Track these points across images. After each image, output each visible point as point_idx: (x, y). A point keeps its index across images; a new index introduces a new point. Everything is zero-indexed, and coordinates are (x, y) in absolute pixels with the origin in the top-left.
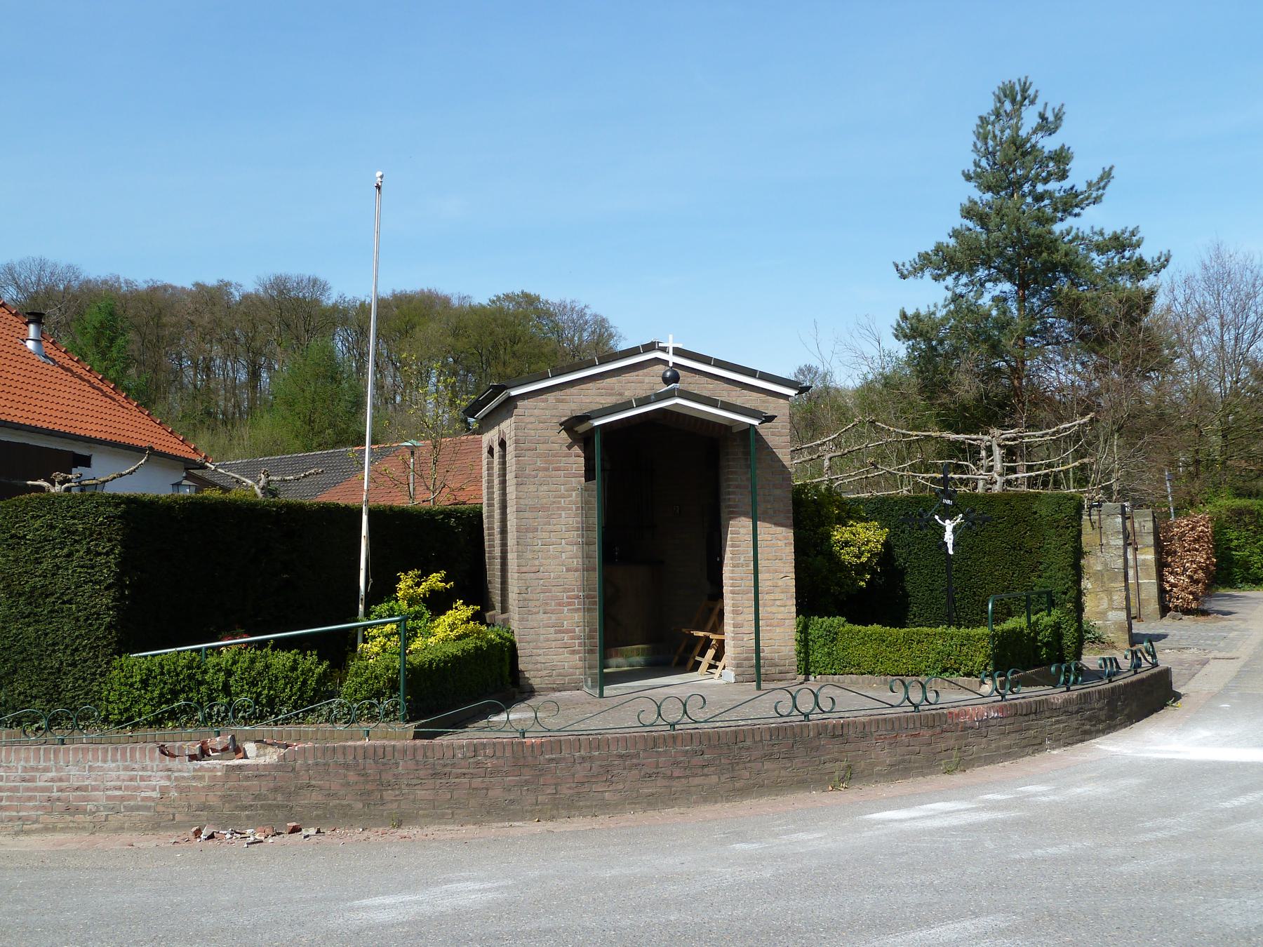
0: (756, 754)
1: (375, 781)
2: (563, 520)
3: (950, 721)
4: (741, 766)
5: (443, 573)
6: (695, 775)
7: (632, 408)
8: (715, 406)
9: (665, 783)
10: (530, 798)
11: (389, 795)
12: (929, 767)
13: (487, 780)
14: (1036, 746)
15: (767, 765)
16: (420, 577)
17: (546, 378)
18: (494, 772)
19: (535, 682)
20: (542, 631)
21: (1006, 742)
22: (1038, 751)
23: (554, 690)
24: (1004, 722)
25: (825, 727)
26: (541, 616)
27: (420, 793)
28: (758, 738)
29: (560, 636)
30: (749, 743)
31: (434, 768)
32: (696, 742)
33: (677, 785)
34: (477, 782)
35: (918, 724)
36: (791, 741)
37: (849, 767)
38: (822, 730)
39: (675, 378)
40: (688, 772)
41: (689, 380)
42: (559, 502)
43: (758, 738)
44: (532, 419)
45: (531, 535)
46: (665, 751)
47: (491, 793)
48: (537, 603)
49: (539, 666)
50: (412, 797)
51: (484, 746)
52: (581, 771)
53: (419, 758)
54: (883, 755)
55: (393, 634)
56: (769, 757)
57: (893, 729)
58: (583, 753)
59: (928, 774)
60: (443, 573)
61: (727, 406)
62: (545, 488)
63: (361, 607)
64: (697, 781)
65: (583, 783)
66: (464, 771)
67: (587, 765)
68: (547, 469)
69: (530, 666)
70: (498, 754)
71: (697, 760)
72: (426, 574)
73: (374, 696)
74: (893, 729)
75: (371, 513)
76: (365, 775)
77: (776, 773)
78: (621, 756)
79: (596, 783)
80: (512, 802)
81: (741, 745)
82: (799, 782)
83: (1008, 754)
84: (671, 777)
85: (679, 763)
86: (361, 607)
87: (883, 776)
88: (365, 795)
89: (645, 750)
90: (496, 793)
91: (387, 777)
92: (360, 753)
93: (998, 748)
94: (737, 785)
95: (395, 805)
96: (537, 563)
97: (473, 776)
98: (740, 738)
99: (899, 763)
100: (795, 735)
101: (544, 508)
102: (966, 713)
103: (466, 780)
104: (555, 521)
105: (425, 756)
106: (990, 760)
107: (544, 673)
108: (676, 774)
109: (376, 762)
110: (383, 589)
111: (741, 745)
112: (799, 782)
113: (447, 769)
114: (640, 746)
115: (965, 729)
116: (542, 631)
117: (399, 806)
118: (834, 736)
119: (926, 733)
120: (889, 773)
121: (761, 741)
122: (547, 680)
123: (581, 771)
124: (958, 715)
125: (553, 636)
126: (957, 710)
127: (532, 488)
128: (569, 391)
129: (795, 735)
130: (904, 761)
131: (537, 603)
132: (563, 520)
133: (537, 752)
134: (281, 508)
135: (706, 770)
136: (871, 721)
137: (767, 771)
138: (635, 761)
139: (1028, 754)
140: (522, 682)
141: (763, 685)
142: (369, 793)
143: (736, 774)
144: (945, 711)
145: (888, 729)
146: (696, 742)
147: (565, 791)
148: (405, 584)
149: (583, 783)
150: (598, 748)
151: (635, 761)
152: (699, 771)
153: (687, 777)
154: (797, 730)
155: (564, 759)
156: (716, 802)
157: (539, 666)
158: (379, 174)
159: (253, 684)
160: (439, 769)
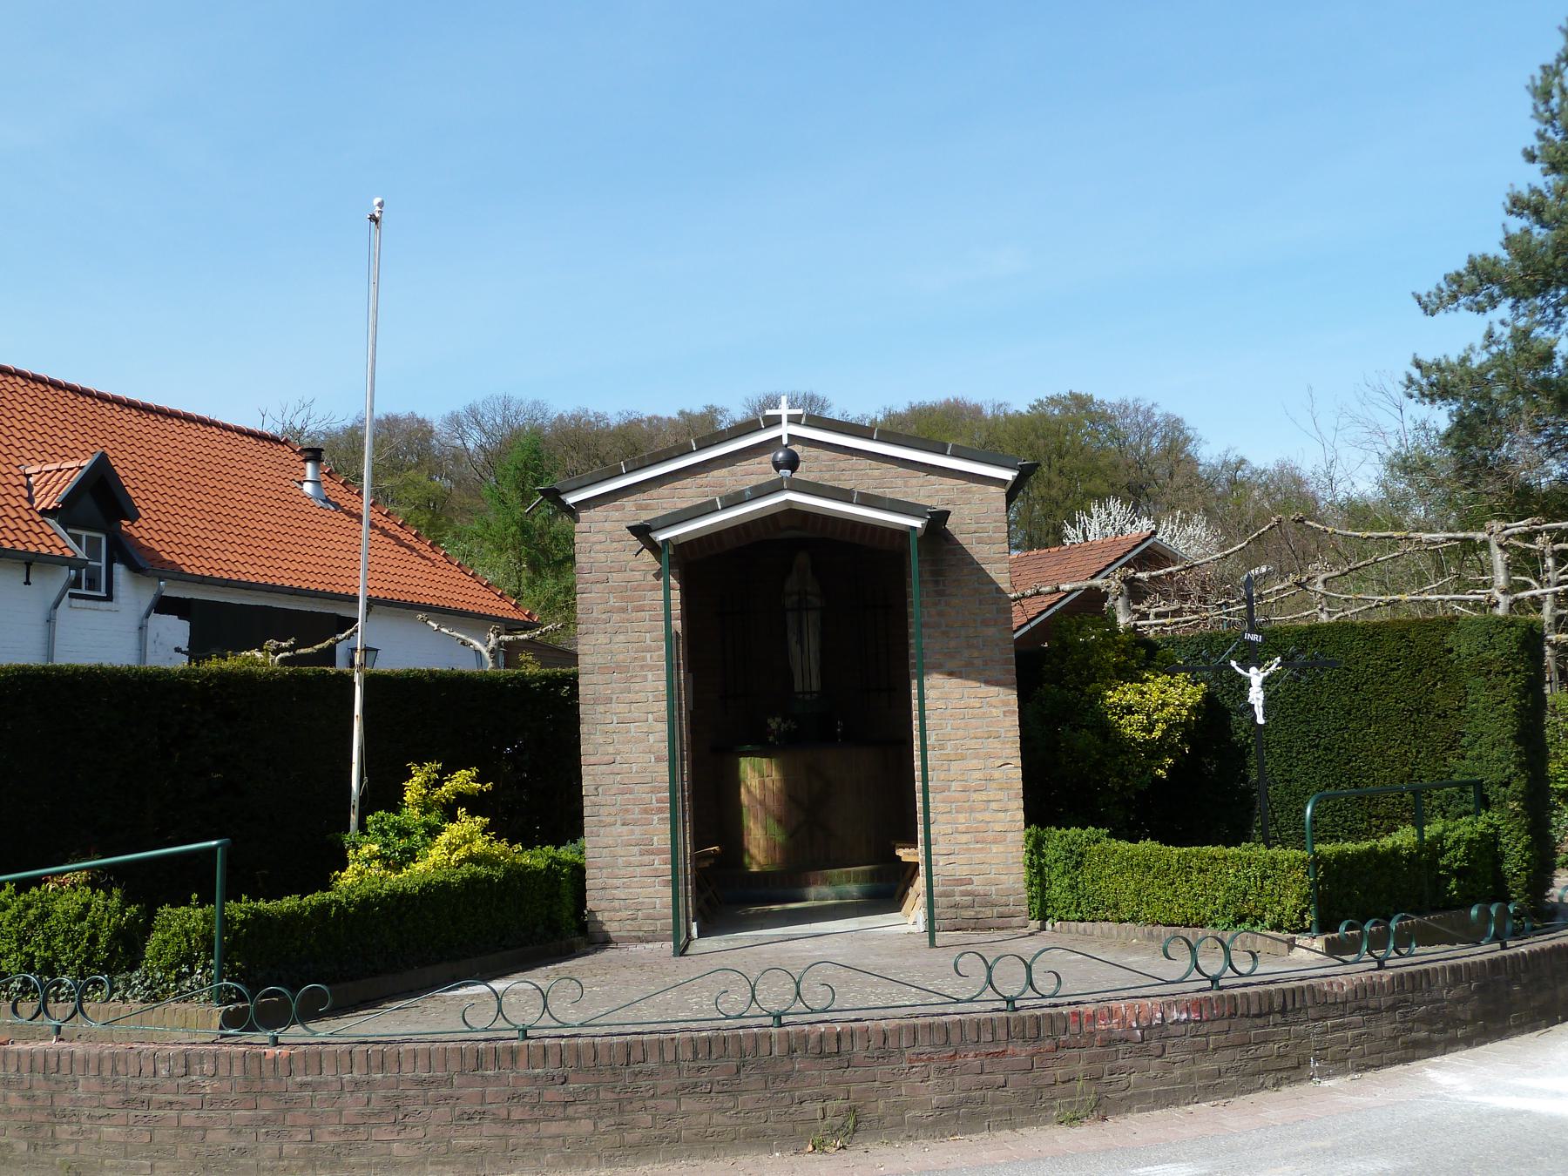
0: (664, 1084)
1: (43, 1108)
2: (650, 685)
3: (1074, 1028)
4: (637, 1105)
5: (474, 771)
6: (552, 1119)
7: (715, 511)
8: (849, 501)
9: (498, 1129)
10: (269, 1148)
11: (64, 1131)
12: (1026, 1112)
13: (203, 1114)
14: (1289, 1070)
15: (687, 1104)
16: (441, 773)
17: (618, 474)
18: (215, 1102)
19: (612, 928)
20: (620, 851)
21: (1207, 1066)
22: (1290, 1081)
23: (641, 940)
24: (1205, 1028)
25: (805, 1037)
26: (619, 829)
27: (108, 1131)
28: (669, 1056)
29: (646, 859)
30: (652, 1063)
31: (126, 1092)
32: (553, 1059)
33: (518, 1135)
34: (189, 1117)
35: (1002, 1034)
36: (734, 1063)
37: (853, 1110)
38: (796, 1046)
39: (792, 462)
40: (538, 1113)
41: (842, 465)
42: (644, 659)
43: (669, 1056)
44: (601, 537)
45: (601, 708)
46: (497, 1077)
47: (210, 1136)
48: (613, 810)
49: (616, 904)
50: (95, 1136)
51: (201, 1057)
52: (352, 1106)
53: (106, 1073)
54: (930, 1092)
55: (374, 857)
56: (690, 1089)
57: (947, 1042)
58: (356, 1074)
59: (1023, 1125)
60: (474, 771)
61: (867, 501)
62: (621, 637)
63: (354, 818)
64: (554, 1128)
65: (356, 1126)
66: (170, 1097)
67: (362, 1096)
68: (624, 610)
69: (604, 905)
70: (222, 1072)
71: (554, 1093)
72: (449, 769)
73: (183, 960)
74: (947, 1042)
75: (372, 682)
76: (32, 1098)
77: (705, 1117)
78: (421, 1082)
79: (378, 1125)
80: (243, 1152)
81: (637, 1068)
82: (748, 1135)
83: (1215, 1087)
84: (507, 1120)
85: (521, 1096)
86: (354, 818)
87: (919, 1126)
88: (32, 1128)
89: (461, 1072)
90: (218, 1136)
91: (62, 1102)
92: (25, 1063)
93: (1189, 1077)
94: (628, 1138)
95: (71, 1149)
96: (611, 749)
97: (184, 1106)
98: (637, 1054)
99: (961, 1104)
100: (742, 1054)
101: (620, 668)
102: (1112, 1014)
103: (173, 1113)
104: (637, 687)
105: (114, 1071)
106: (1168, 1098)
107: (624, 914)
108: (515, 1116)
109: (47, 1079)
110: (385, 794)
111: (637, 1068)
112: (748, 1135)
113: (145, 1094)
114: (454, 1066)
115: (1109, 1042)
116: (620, 851)
117: (76, 1152)
118: (821, 1055)
119: (1021, 1051)
120: (935, 1124)
121: (676, 1060)
122: (628, 925)
123: (352, 1106)
124: (1092, 1018)
125: (636, 859)
126: (1091, 1008)
127: (602, 639)
128: (655, 493)
129: (742, 1054)
130: (968, 1101)
131: (613, 810)
132: (650, 685)
133: (282, 1071)
134: (209, 679)
135: (570, 1111)
136: (900, 1028)
137: (686, 1115)
138: (444, 1091)
139: (1263, 1087)
140: (591, 928)
141: (941, 938)
142: (38, 1127)
143: (628, 1117)
144: (1065, 1010)
145: (943, 1041)
146: (553, 1059)
147: (326, 1138)
148: (413, 789)
149: (356, 1126)
150: (382, 1067)
151: (444, 1091)
152: (559, 1112)
153: (536, 1121)
154: (748, 1045)
155: (326, 1083)
156: (588, 1166)
157: (616, 904)
158: (377, 200)
159: (23, 940)
160: (134, 1093)
